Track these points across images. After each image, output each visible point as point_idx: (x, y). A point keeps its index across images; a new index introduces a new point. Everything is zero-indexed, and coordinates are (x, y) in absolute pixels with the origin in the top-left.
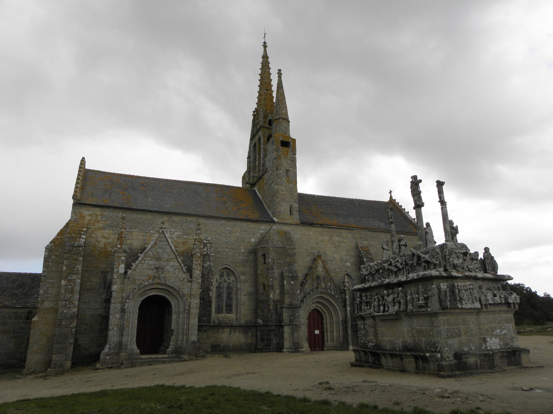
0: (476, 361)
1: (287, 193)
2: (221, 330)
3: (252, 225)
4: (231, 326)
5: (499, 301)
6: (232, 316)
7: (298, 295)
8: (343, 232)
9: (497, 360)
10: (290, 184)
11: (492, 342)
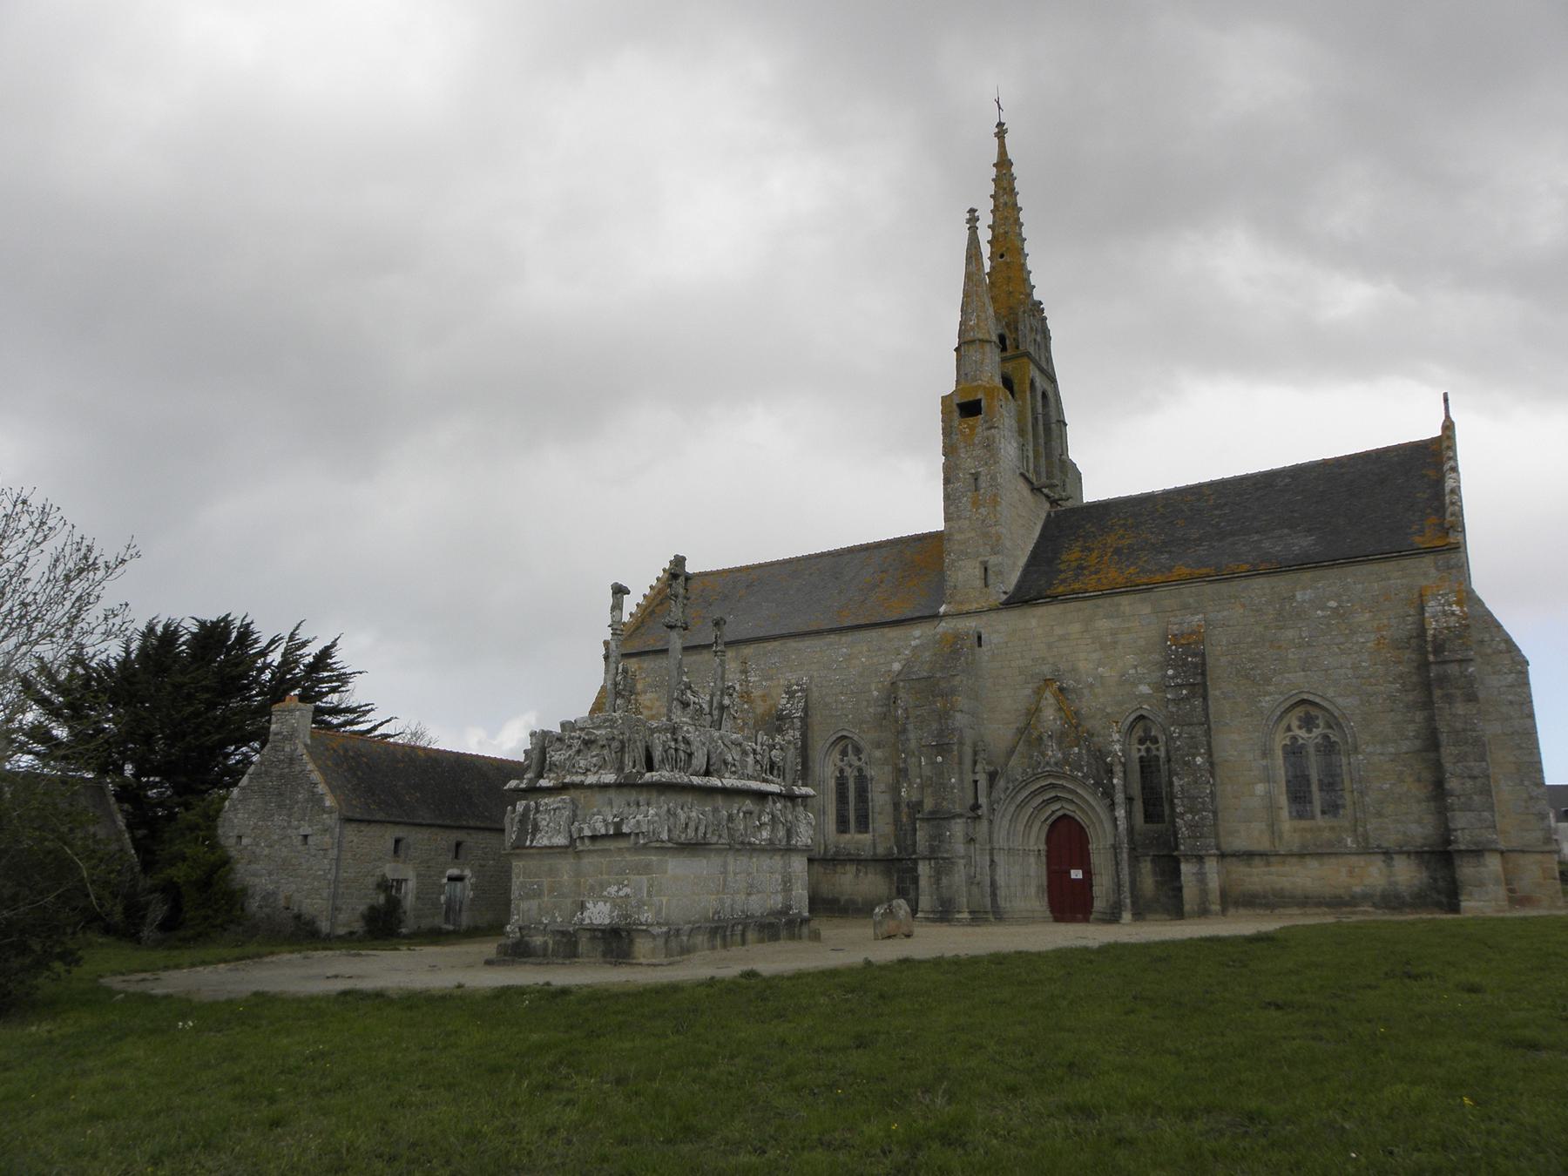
0: (546, 943)
1: (973, 534)
2: (839, 869)
3: (892, 633)
4: (858, 861)
5: (603, 831)
6: (866, 838)
7: (953, 787)
8: (1125, 602)
9: (584, 944)
10: (982, 510)
11: (596, 911)
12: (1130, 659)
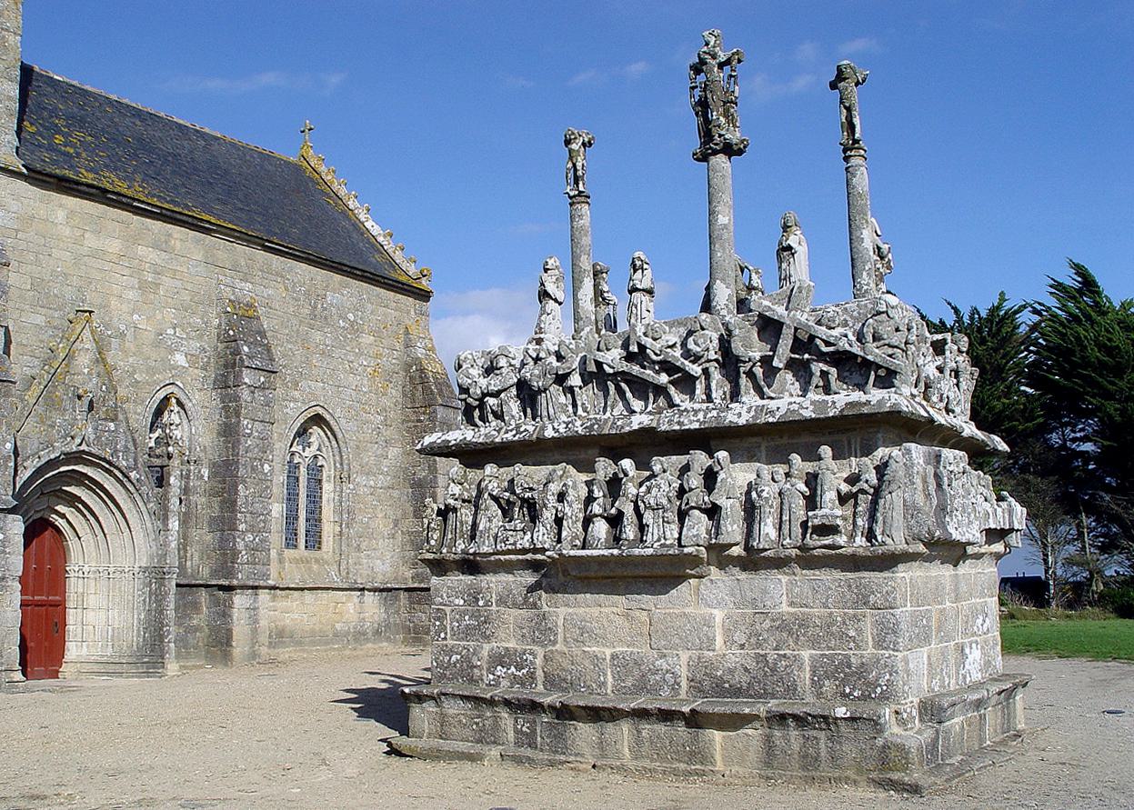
12: (170, 314)
